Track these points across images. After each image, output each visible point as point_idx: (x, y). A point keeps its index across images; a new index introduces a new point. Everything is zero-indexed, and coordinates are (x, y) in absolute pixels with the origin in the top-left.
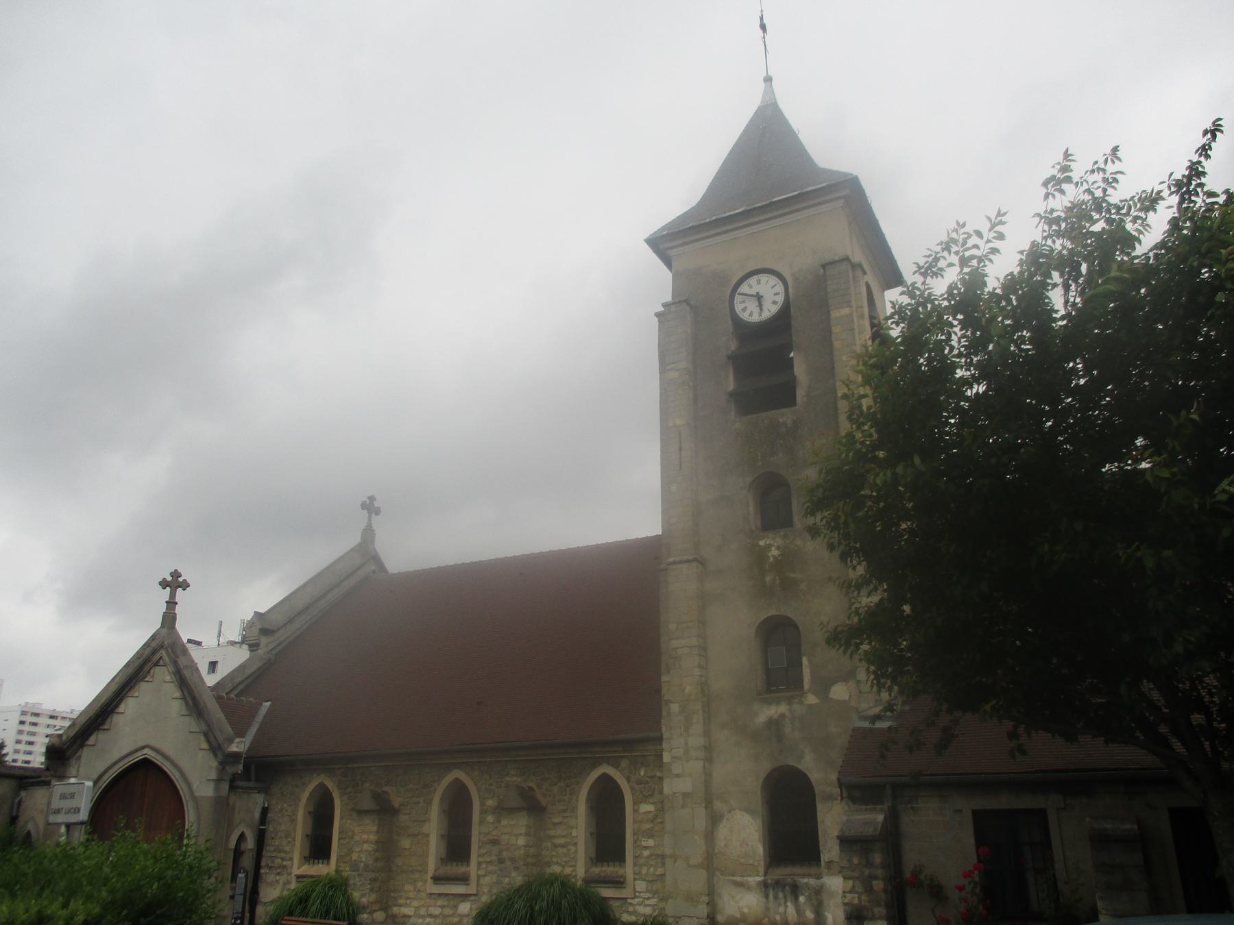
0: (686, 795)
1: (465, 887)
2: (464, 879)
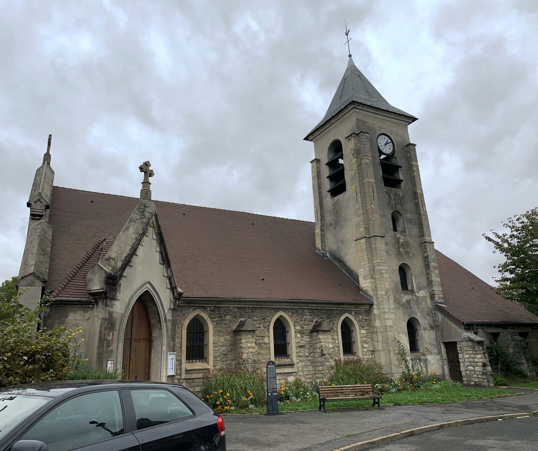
0: (391, 327)
1: (291, 369)
2: (292, 365)
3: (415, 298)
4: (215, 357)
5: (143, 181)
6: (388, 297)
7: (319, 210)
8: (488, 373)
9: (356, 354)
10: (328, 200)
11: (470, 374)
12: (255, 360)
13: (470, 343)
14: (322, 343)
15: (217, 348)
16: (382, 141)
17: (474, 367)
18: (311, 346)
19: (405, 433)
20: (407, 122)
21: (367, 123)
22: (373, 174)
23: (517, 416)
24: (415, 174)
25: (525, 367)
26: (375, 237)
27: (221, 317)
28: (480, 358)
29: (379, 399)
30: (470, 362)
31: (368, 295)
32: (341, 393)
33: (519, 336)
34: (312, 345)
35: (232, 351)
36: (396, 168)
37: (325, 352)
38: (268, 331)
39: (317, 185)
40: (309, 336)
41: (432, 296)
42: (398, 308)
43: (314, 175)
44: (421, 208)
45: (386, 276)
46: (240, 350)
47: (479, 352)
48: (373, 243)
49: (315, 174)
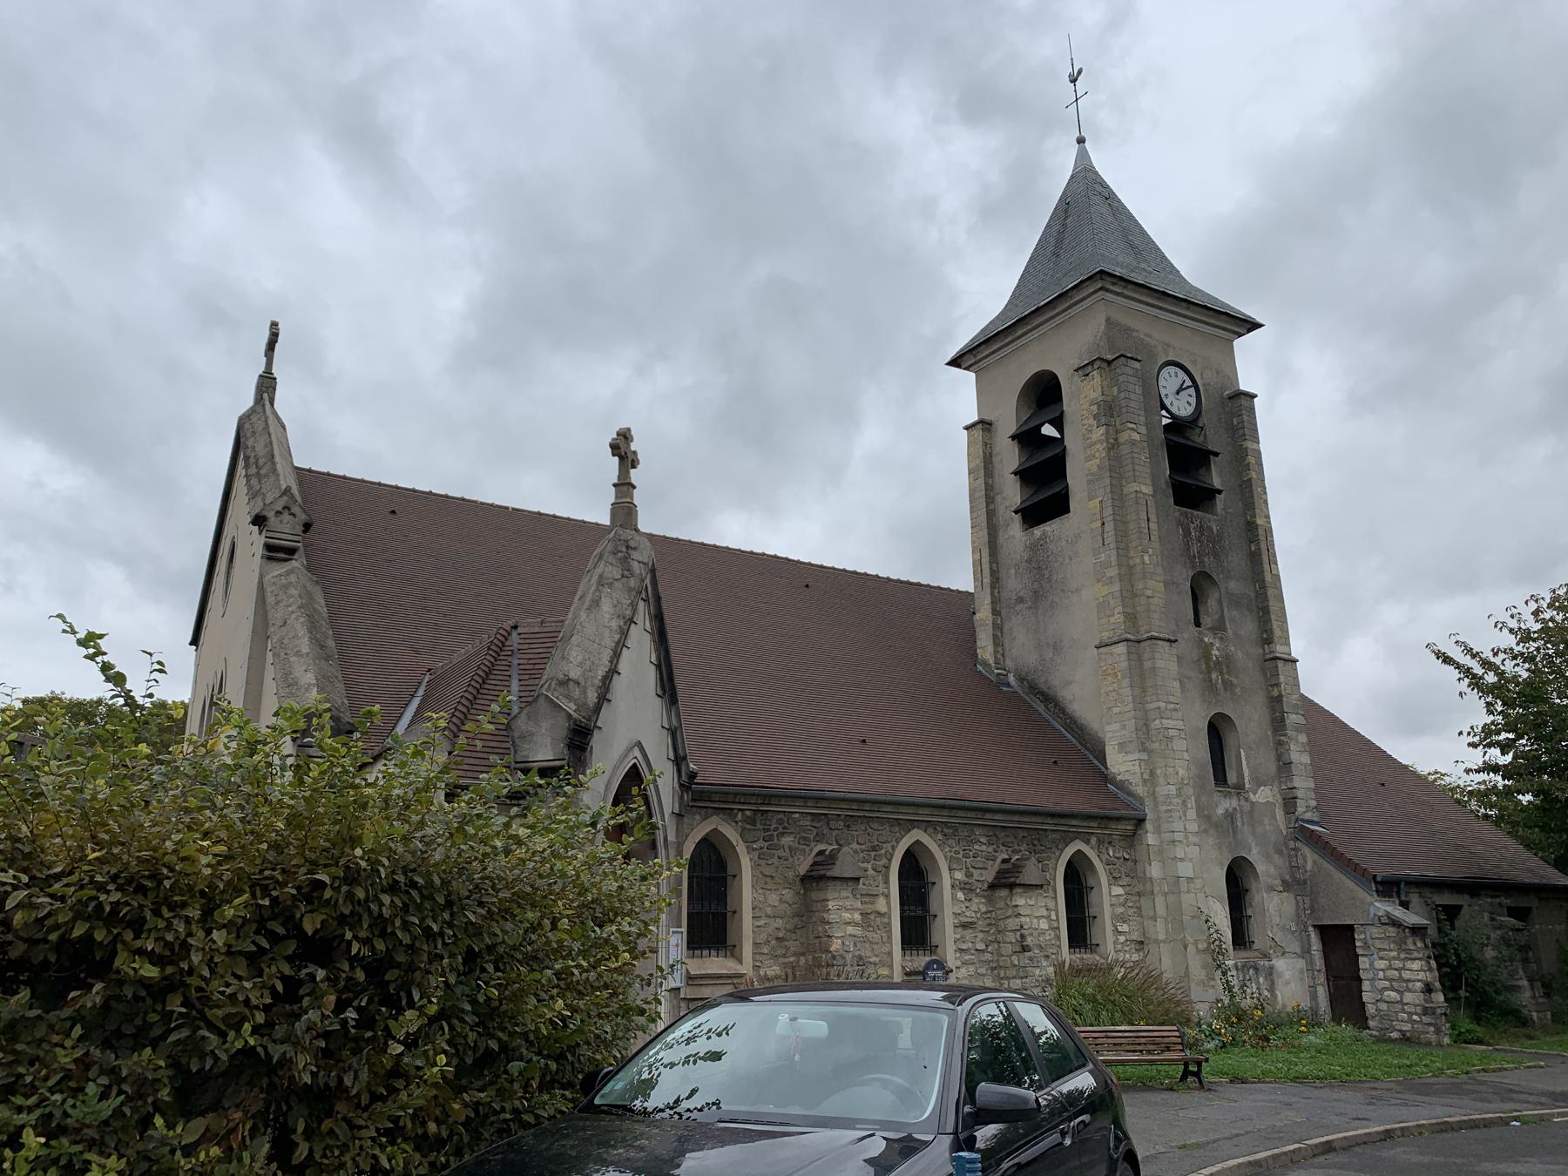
3: (1246, 807)
4: (756, 944)
5: (616, 481)
6: (1184, 802)
7: (986, 560)
8: (1439, 1011)
9: (1098, 949)
10: (1015, 535)
11: (1389, 1010)
12: (860, 958)
13: (1392, 931)
14: (1023, 919)
15: (762, 922)
16: (1170, 381)
17: (1400, 993)
18: (990, 924)
19: (1316, 1146)
20: (1235, 333)
21: (1134, 330)
22: (1148, 471)
23: (1553, 1115)
24: (1254, 475)
25: (1525, 996)
26: (1154, 641)
27: (770, 838)
28: (1419, 970)
29: (1199, 1064)
30: (1391, 980)
31: (1130, 794)
32: (1115, 1044)
33: (1509, 916)
34: (995, 926)
35: (798, 931)
36: (1203, 457)
37: (1029, 941)
38: (887, 882)
39: (984, 492)
40: (985, 897)
41: (1289, 803)
42: (1205, 831)
43: (973, 465)
44: (1266, 567)
45: (1180, 745)
46: (820, 928)
47: (1415, 954)
48: (1146, 656)
49: (979, 462)
